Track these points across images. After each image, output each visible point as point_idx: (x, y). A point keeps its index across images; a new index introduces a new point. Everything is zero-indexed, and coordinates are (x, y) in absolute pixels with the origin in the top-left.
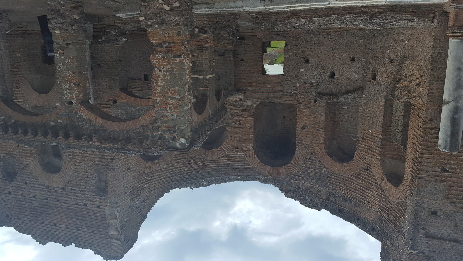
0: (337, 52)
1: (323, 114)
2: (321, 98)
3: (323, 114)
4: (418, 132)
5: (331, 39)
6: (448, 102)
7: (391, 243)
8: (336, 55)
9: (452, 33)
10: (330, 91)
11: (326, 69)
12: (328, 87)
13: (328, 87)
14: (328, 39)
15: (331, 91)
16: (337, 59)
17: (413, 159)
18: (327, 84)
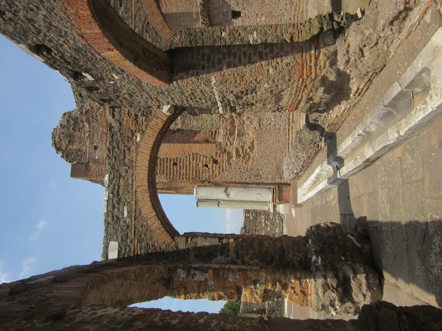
0: (267, 20)
1: (180, 9)
2: (203, 10)
3: (180, 9)
4: (201, 165)
5: (286, 9)
6: (228, 198)
7: (90, 132)
8: (263, 19)
9: (275, 199)
10: (214, 16)
11: (243, 5)
12: (219, 12)
13: (219, 12)
14: (286, 4)
15: (215, 17)
16: (258, 20)
17: (177, 158)
18: (223, 10)
